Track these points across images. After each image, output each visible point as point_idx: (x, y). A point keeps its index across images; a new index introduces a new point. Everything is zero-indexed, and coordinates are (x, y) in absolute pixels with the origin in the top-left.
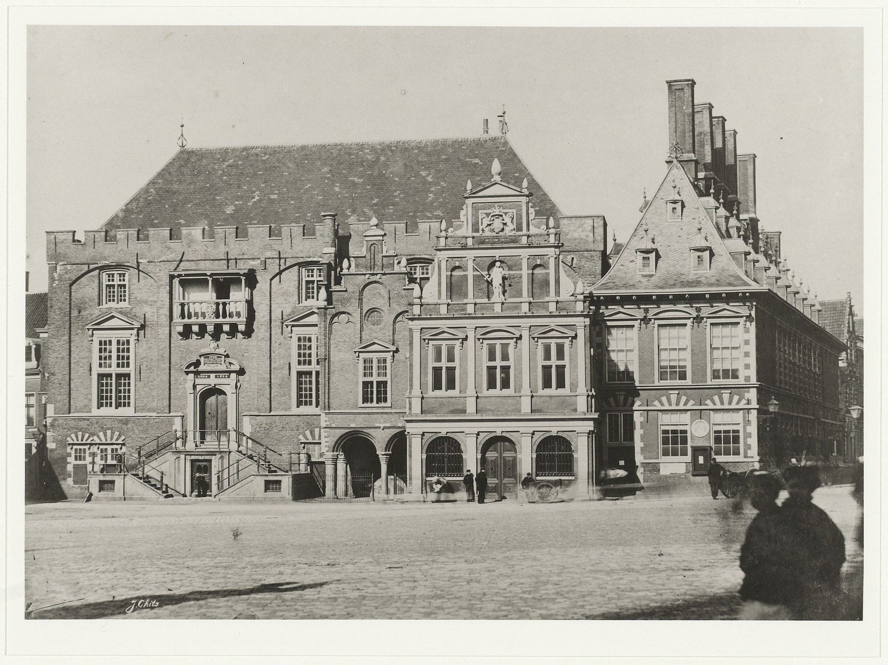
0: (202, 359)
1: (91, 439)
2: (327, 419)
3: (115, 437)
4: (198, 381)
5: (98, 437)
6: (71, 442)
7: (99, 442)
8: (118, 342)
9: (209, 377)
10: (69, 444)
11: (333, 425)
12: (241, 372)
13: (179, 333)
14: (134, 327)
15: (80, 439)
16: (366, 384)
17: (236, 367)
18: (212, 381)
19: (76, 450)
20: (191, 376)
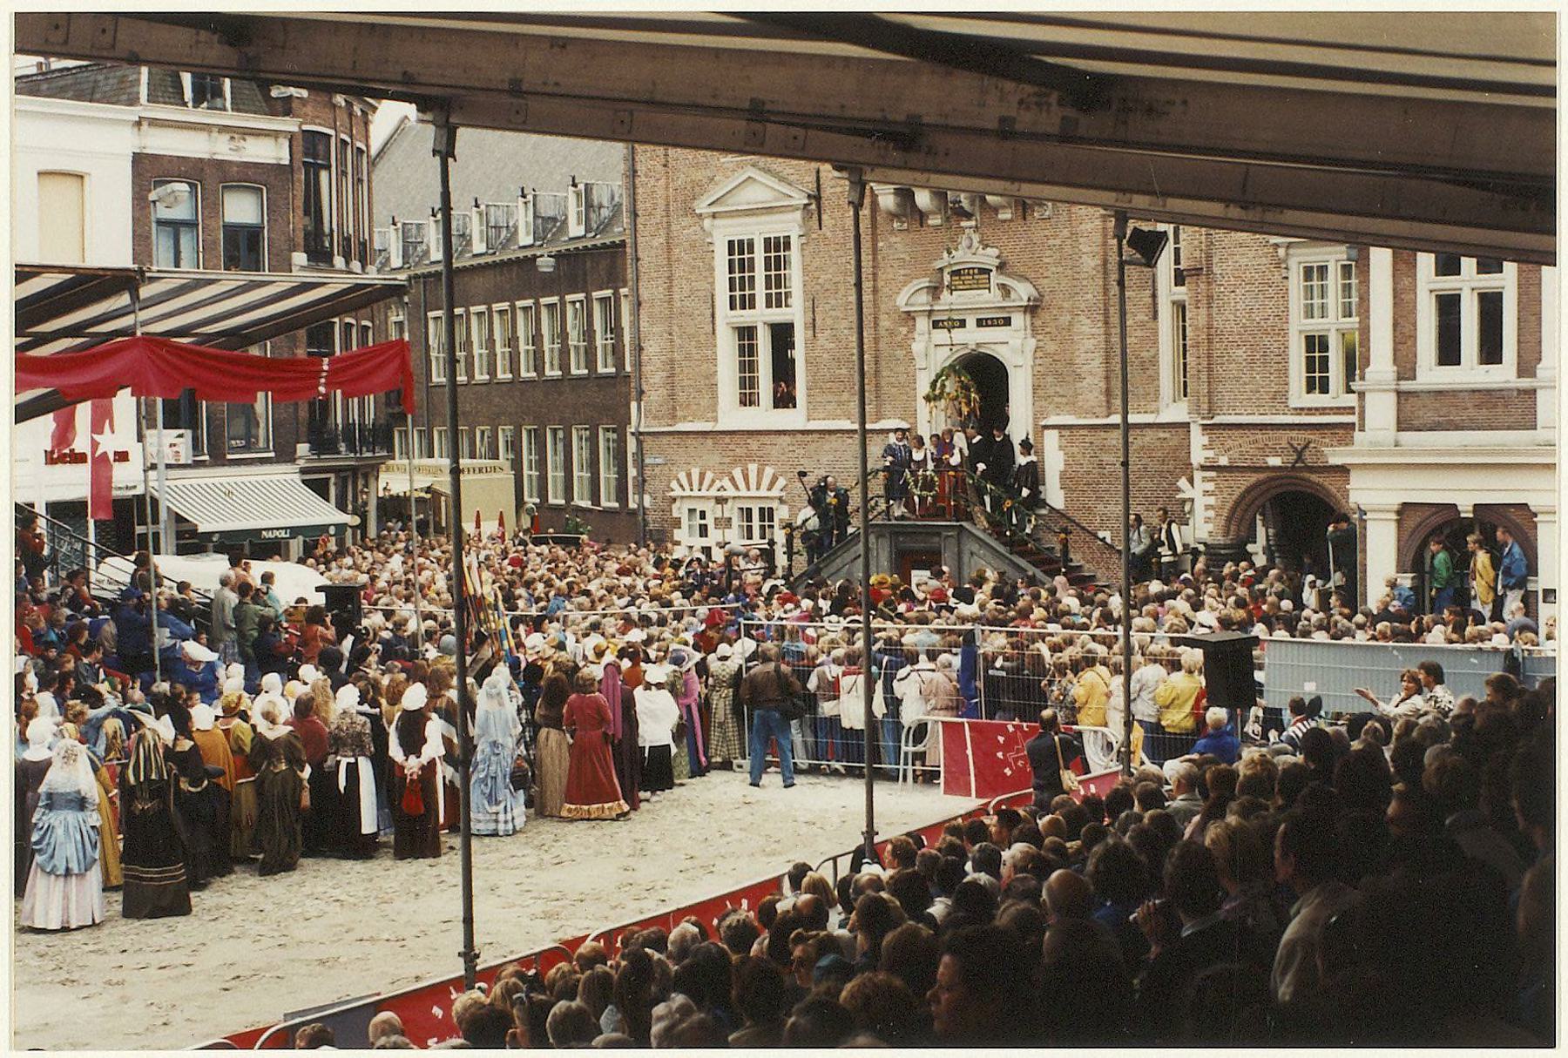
0: (947, 278)
1: (718, 484)
2: (1205, 440)
3: (766, 482)
4: (941, 336)
5: (732, 480)
6: (678, 492)
7: (731, 492)
8: (767, 241)
9: (963, 324)
10: (674, 500)
11: (1224, 461)
12: (1032, 309)
13: (893, 216)
14: (793, 202)
15: (696, 485)
16: (1316, 344)
17: (1023, 291)
18: (972, 337)
19: (692, 511)
20: (922, 324)
